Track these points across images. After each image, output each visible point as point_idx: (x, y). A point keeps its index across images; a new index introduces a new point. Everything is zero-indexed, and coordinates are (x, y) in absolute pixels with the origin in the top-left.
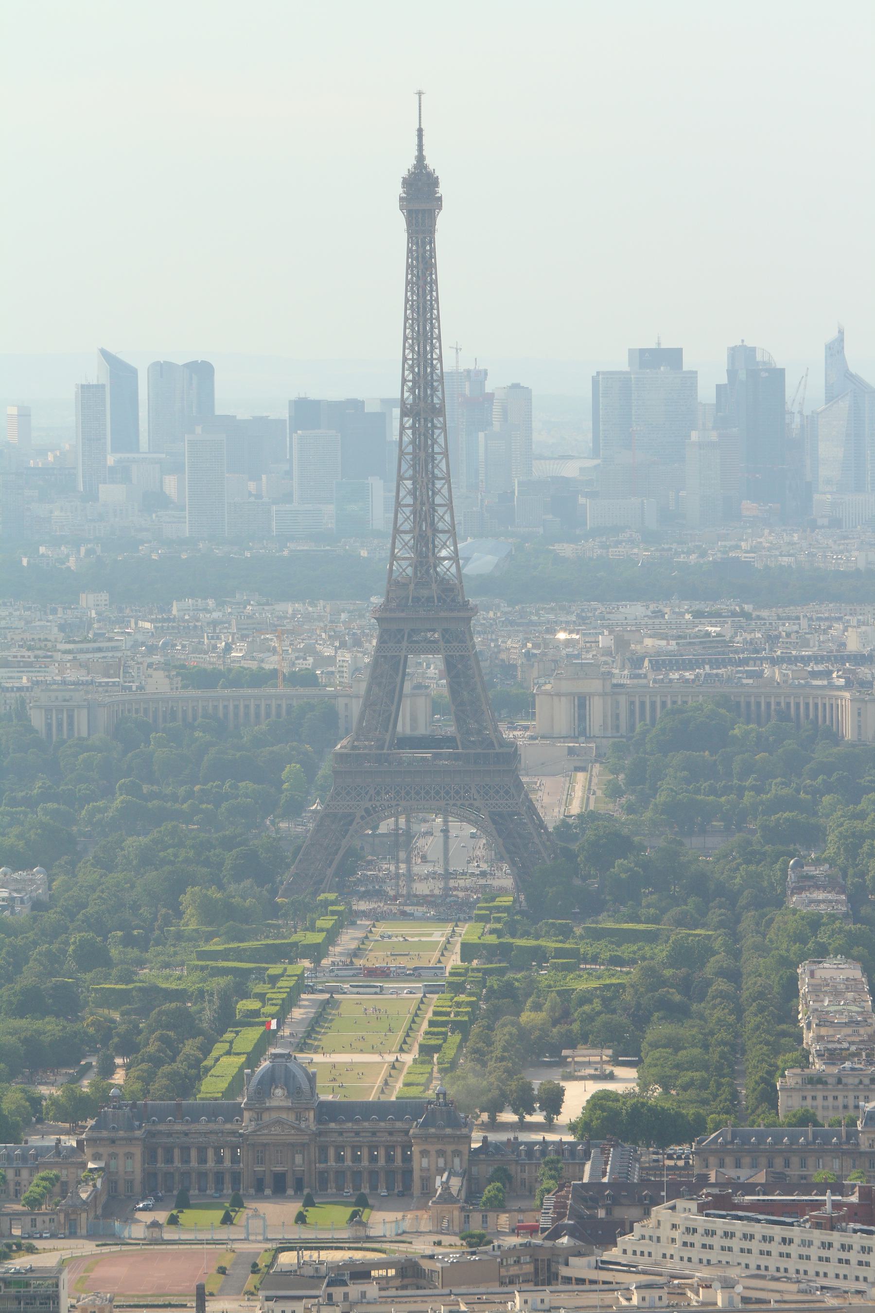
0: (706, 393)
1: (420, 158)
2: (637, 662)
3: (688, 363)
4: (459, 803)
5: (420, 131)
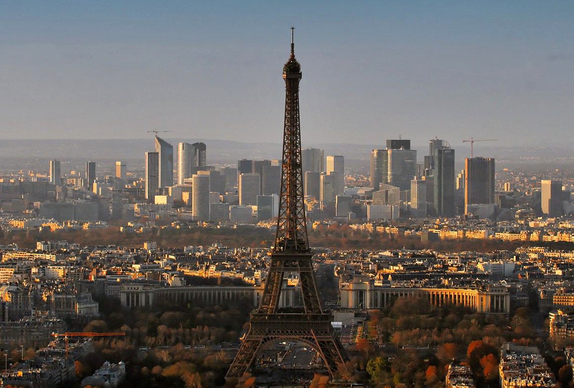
0: (420, 160)
1: (293, 56)
2: (386, 276)
3: (413, 146)
4: (305, 337)
5: (293, 45)
